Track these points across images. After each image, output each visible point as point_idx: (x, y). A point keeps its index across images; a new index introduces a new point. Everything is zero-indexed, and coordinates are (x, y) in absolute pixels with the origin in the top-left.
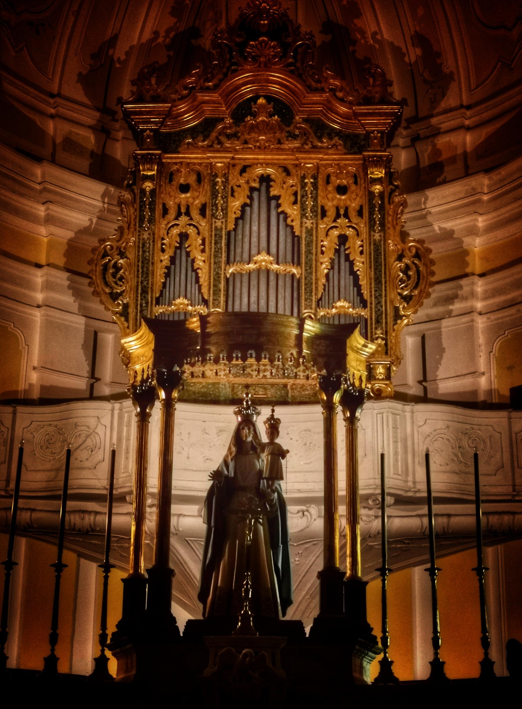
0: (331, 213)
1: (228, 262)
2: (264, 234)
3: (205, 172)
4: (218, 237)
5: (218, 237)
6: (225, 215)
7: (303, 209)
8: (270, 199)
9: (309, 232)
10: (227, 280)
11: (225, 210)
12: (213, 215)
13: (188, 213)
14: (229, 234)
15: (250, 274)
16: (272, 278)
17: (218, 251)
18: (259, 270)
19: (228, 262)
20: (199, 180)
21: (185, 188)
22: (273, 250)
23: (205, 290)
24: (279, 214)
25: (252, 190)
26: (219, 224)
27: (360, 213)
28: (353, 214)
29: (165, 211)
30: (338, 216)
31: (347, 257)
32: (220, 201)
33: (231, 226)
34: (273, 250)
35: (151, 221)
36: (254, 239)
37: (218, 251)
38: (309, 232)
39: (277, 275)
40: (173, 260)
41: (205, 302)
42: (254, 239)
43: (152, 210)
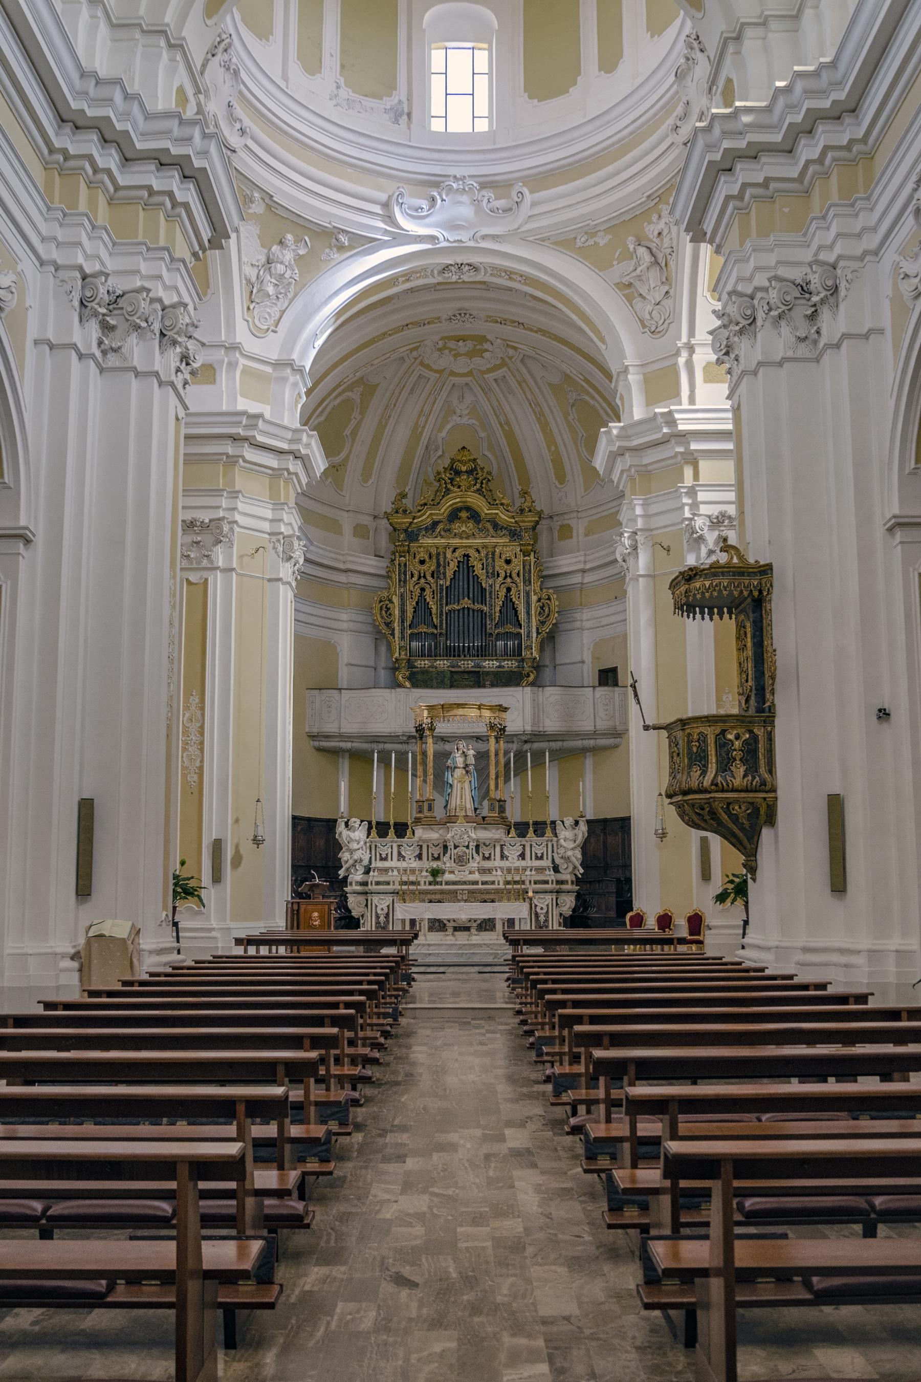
0: (503, 574)
1: (447, 605)
2: (466, 586)
3: (434, 551)
4: (442, 590)
5: (442, 590)
6: (445, 577)
7: (487, 573)
8: (468, 567)
9: (491, 586)
10: (447, 614)
11: (444, 574)
12: (438, 577)
13: (424, 577)
14: (447, 588)
15: (459, 610)
16: (471, 612)
17: (441, 598)
18: (464, 608)
19: (447, 605)
20: (430, 557)
21: (422, 562)
22: (471, 596)
23: (435, 620)
24: (473, 577)
25: (459, 562)
26: (441, 582)
27: (518, 575)
28: (514, 575)
29: (412, 576)
30: (506, 577)
31: (511, 600)
32: (441, 568)
33: (448, 583)
34: (471, 596)
35: (405, 582)
36: (461, 590)
37: (441, 598)
38: (491, 586)
39: (473, 610)
40: (417, 603)
41: (436, 627)
42: (461, 590)
43: (405, 575)
